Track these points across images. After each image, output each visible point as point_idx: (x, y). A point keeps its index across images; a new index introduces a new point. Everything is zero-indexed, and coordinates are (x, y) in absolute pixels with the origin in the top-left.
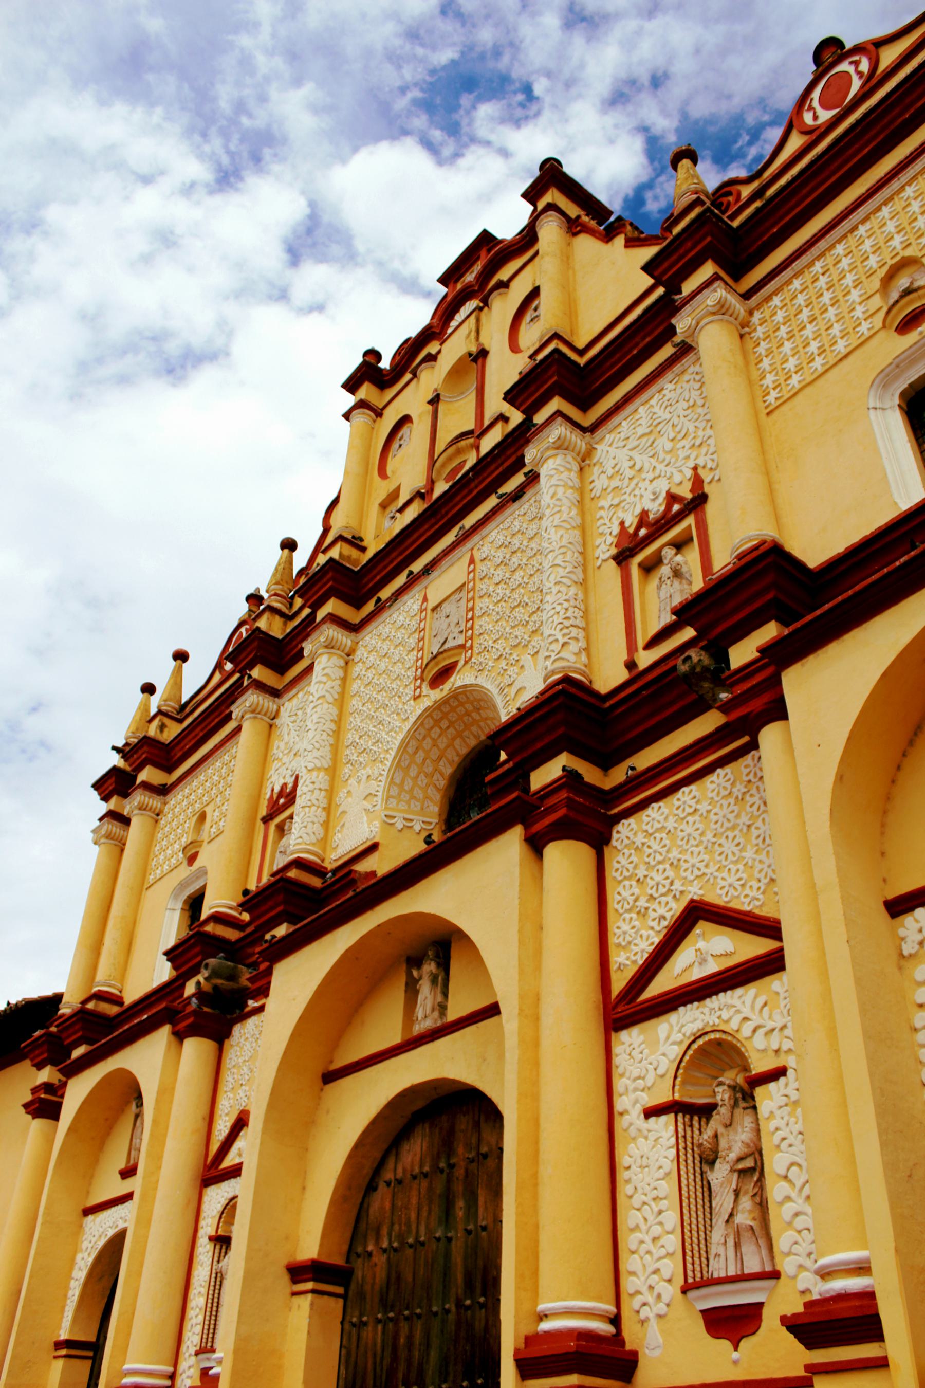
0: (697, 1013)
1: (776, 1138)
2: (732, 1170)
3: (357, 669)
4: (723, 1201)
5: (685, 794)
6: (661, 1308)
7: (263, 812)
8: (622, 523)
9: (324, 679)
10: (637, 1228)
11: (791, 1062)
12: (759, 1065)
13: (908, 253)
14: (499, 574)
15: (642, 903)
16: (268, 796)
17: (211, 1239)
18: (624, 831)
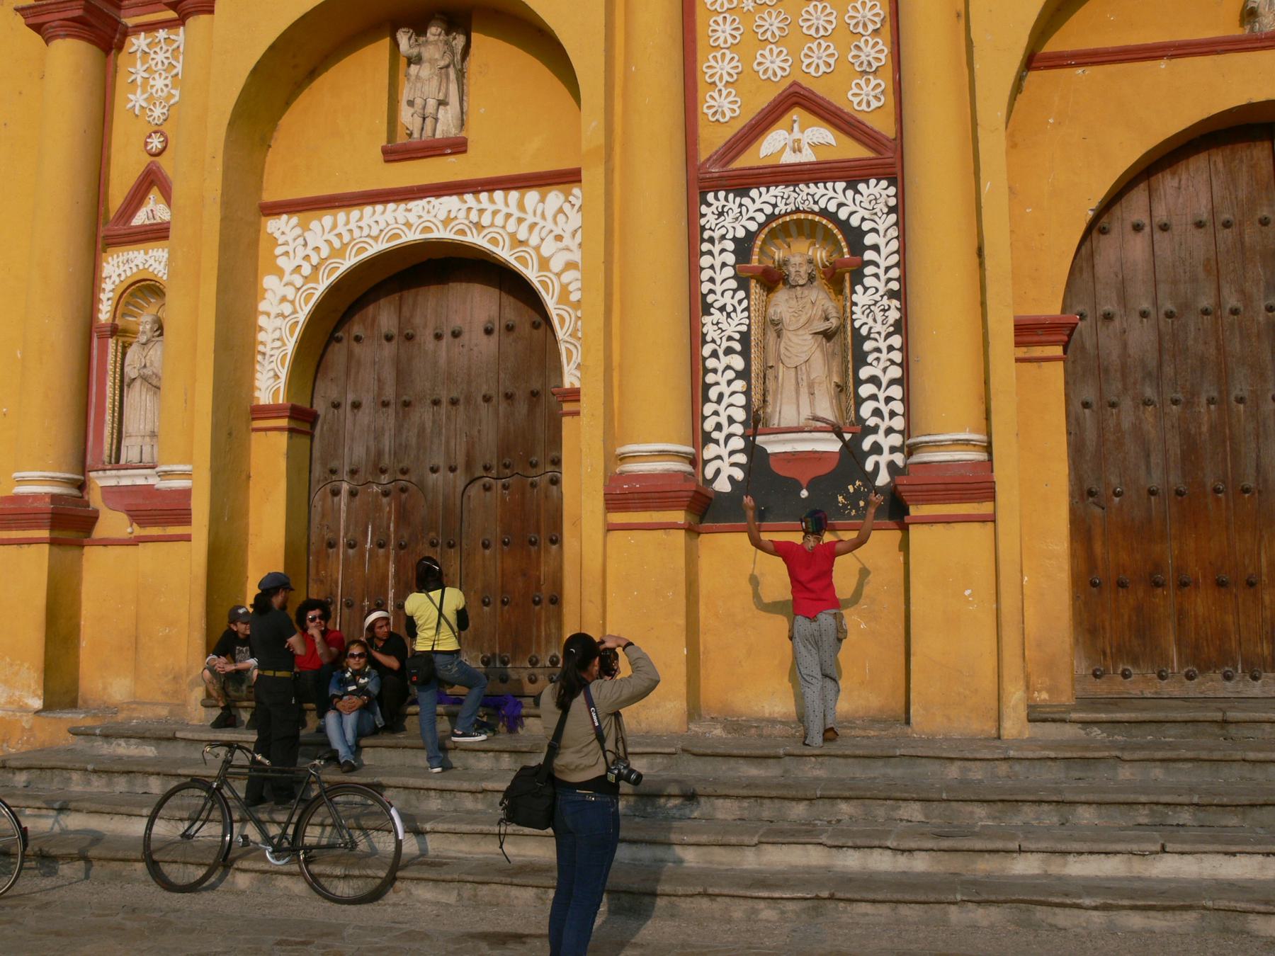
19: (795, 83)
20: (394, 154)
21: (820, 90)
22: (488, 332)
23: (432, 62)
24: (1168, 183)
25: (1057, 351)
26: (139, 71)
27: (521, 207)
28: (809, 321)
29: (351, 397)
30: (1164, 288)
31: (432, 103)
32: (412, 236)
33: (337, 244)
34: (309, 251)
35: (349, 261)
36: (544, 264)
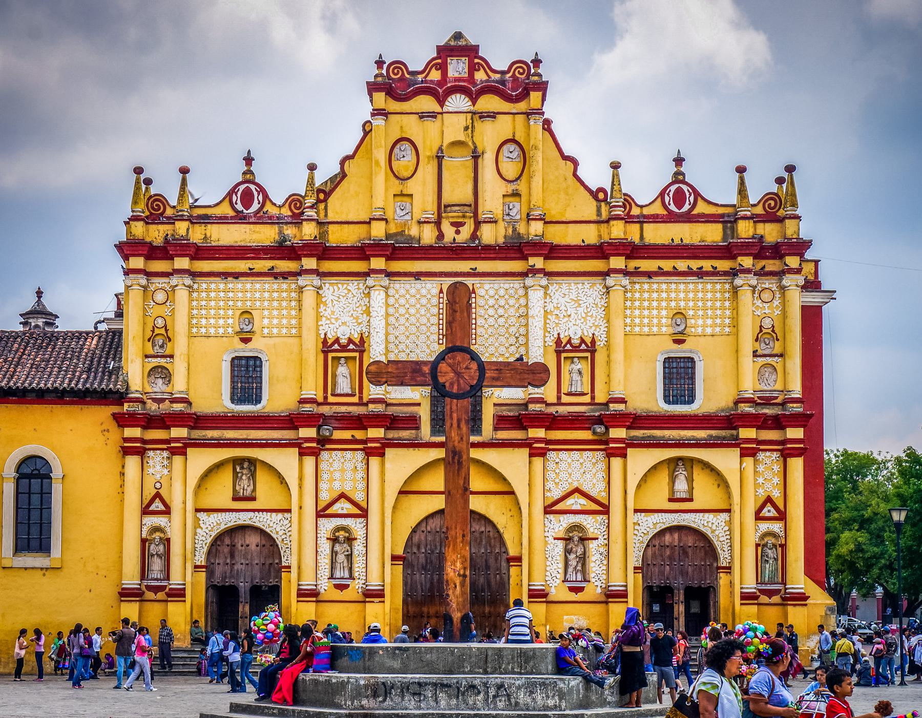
0: (573, 517)
1: (593, 553)
2: (577, 556)
3: (391, 301)
4: (573, 563)
5: (576, 454)
6: (556, 585)
7: (321, 346)
8: (559, 334)
9: (382, 305)
10: (550, 566)
11: (600, 537)
12: (591, 536)
13: (684, 312)
14: (491, 312)
15: (557, 481)
16: (323, 336)
17: (328, 539)
18: (552, 455)
19: (343, 492)
20: (235, 499)
21: (349, 495)
22: (257, 546)
23: (246, 475)
24: (431, 521)
25: (402, 563)
26: (151, 462)
27: (271, 516)
28: (344, 552)
29: (217, 561)
30: (429, 547)
31: (246, 486)
32: (240, 522)
33: (219, 522)
34: (210, 523)
35: (223, 527)
36: (277, 533)
